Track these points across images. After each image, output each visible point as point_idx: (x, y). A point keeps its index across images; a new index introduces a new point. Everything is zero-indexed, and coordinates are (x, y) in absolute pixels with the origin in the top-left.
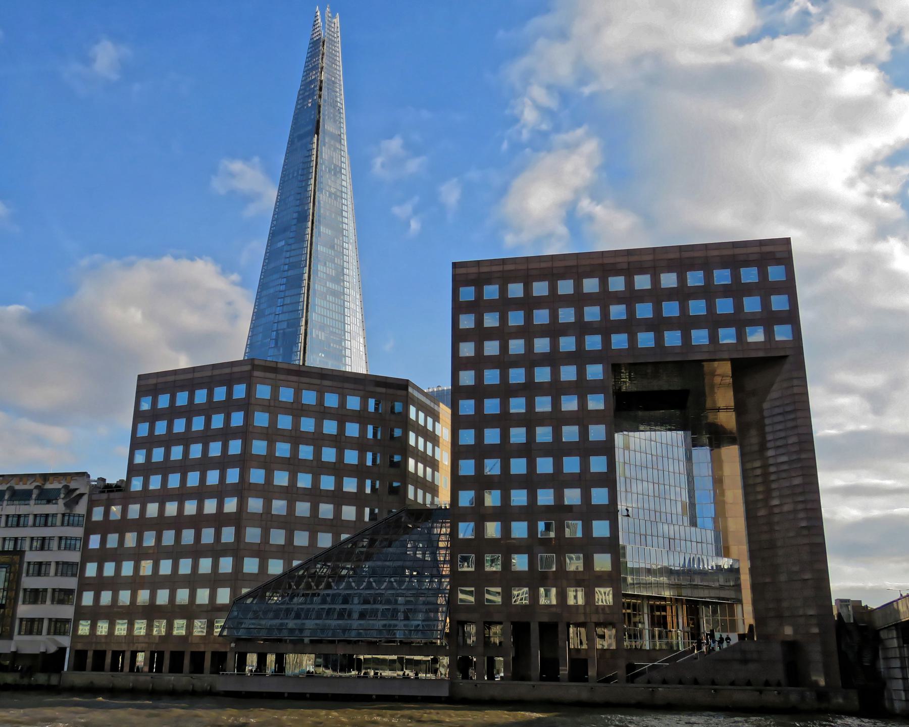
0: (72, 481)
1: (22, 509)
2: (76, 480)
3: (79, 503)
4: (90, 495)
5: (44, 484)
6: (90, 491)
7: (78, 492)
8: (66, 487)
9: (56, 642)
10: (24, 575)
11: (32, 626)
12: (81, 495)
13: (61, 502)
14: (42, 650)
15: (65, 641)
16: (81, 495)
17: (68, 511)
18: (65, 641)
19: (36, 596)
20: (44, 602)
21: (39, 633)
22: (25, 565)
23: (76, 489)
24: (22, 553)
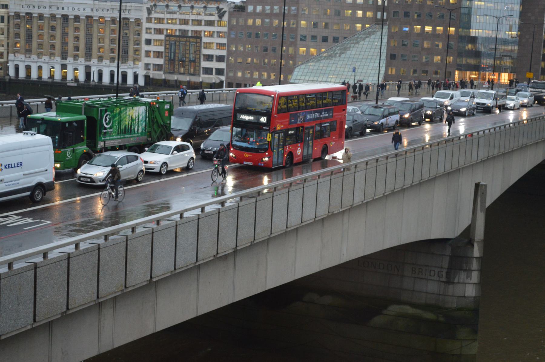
0: (220, 5)
1: (199, 18)
2: (222, 4)
3: (225, 16)
4: (229, 12)
5: (207, 5)
6: (229, 10)
7: (223, 10)
8: (218, 8)
9: (219, 78)
10: (202, 48)
11: (208, 71)
12: (225, 12)
13: (216, 15)
14: (214, 81)
15: (223, 78)
16: (225, 12)
17: (220, 20)
18: (223, 78)
19: (209, 58)
20: (213, 61)
21: (212, 74)
22: (203, 44)
23: (222, 9)
24: (200, 38)
